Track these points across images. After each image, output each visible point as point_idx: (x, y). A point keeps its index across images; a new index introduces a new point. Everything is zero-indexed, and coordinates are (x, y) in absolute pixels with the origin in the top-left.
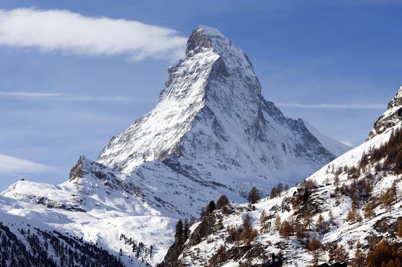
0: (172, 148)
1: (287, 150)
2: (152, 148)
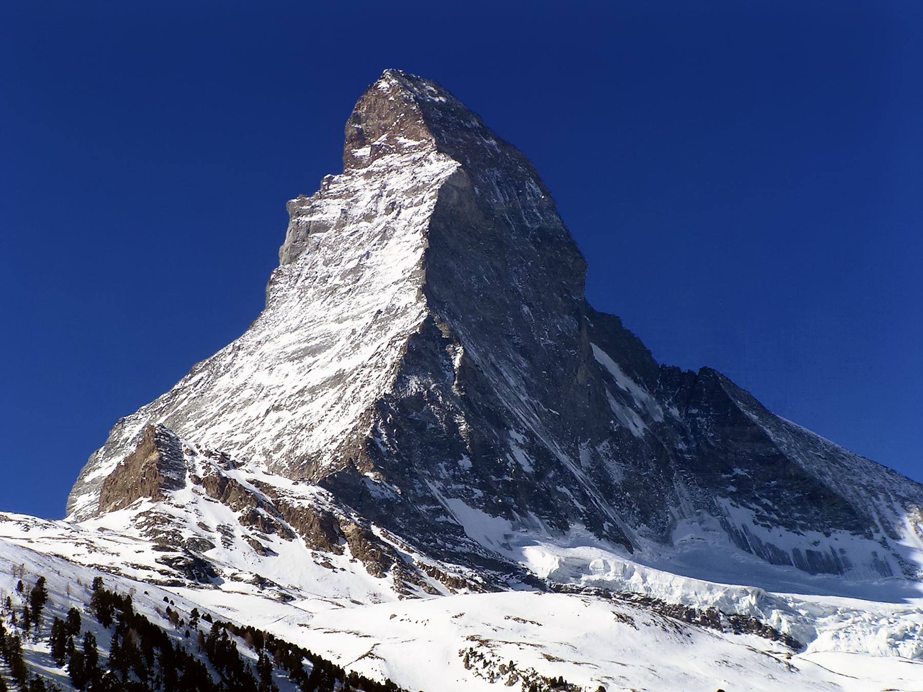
0: (335, 445)
1: (672, 464)
2: (259, 449)
